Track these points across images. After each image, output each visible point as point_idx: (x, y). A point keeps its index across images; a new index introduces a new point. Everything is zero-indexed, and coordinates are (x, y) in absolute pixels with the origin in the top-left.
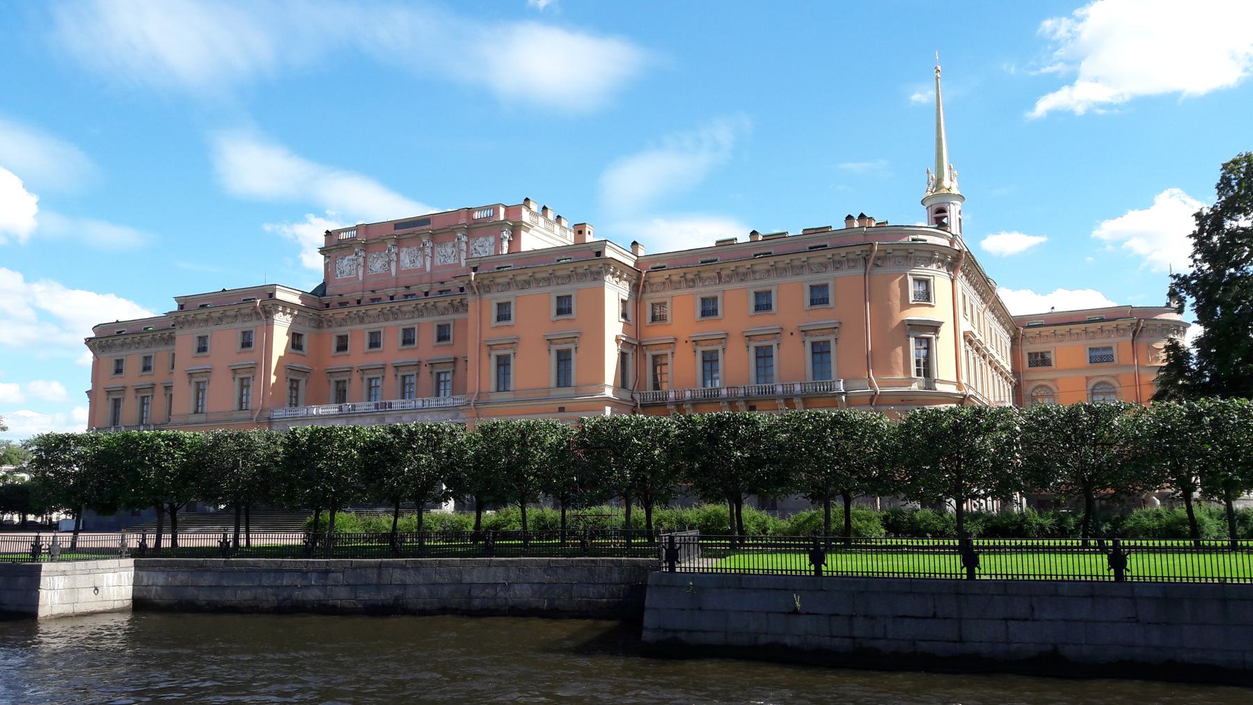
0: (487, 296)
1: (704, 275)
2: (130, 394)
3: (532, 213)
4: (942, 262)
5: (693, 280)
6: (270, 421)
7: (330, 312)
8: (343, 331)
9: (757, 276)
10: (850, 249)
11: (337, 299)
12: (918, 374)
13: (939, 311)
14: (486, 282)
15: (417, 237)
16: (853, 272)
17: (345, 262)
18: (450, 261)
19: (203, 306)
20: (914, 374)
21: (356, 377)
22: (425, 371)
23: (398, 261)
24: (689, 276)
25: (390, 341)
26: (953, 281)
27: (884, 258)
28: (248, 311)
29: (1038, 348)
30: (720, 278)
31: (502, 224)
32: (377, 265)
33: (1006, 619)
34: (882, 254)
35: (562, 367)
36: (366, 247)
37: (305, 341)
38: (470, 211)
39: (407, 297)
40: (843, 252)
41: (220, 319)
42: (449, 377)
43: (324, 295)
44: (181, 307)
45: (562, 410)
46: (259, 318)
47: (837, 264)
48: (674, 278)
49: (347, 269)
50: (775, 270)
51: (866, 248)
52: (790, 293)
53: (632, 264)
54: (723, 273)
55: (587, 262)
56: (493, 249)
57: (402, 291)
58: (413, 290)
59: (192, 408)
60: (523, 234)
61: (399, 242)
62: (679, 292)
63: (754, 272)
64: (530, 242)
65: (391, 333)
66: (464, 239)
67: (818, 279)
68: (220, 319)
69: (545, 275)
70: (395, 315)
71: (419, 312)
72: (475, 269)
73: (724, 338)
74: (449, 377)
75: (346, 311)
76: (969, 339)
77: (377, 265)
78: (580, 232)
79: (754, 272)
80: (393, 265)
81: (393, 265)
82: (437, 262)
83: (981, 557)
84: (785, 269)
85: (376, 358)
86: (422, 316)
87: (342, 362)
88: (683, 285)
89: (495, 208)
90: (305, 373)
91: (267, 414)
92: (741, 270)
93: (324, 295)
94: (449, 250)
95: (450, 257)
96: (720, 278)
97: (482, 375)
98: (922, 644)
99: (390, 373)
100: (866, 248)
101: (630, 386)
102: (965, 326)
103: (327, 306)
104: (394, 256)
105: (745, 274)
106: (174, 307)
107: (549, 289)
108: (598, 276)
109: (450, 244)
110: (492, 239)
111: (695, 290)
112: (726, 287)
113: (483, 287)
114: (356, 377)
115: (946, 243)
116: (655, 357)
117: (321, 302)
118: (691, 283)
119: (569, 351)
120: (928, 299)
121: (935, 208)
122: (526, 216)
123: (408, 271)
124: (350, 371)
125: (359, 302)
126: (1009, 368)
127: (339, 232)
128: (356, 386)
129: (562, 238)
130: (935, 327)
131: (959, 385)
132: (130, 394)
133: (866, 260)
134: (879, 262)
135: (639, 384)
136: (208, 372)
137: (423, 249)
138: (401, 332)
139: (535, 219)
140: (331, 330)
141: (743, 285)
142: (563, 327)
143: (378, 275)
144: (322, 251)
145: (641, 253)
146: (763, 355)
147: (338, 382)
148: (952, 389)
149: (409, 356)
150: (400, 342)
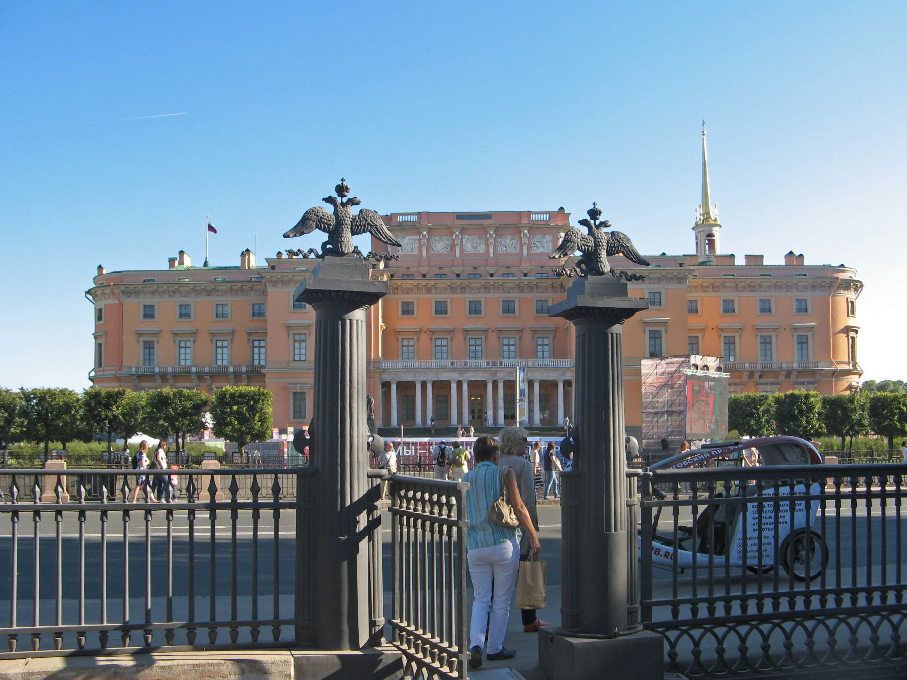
9: (763, 289)
11: (402, 271)
18: (511, 250)
24: (716, 284)
38: (529, 213)
44: (273, 268)
50: (777, 287)
57: (470, 270)
61: (463, 231)
62: (707, 294)
65: (458, 302)
70: (463, 289)
71: (487, 288)
77: (440, 246)
85: (441, 323)
86: (489, 292)
109: (509, 237)
111: (719, 294)
112: (741, 294)
118: (716, 288)
123: (470, 255)
140: (397, 296)
143: (441, 255)
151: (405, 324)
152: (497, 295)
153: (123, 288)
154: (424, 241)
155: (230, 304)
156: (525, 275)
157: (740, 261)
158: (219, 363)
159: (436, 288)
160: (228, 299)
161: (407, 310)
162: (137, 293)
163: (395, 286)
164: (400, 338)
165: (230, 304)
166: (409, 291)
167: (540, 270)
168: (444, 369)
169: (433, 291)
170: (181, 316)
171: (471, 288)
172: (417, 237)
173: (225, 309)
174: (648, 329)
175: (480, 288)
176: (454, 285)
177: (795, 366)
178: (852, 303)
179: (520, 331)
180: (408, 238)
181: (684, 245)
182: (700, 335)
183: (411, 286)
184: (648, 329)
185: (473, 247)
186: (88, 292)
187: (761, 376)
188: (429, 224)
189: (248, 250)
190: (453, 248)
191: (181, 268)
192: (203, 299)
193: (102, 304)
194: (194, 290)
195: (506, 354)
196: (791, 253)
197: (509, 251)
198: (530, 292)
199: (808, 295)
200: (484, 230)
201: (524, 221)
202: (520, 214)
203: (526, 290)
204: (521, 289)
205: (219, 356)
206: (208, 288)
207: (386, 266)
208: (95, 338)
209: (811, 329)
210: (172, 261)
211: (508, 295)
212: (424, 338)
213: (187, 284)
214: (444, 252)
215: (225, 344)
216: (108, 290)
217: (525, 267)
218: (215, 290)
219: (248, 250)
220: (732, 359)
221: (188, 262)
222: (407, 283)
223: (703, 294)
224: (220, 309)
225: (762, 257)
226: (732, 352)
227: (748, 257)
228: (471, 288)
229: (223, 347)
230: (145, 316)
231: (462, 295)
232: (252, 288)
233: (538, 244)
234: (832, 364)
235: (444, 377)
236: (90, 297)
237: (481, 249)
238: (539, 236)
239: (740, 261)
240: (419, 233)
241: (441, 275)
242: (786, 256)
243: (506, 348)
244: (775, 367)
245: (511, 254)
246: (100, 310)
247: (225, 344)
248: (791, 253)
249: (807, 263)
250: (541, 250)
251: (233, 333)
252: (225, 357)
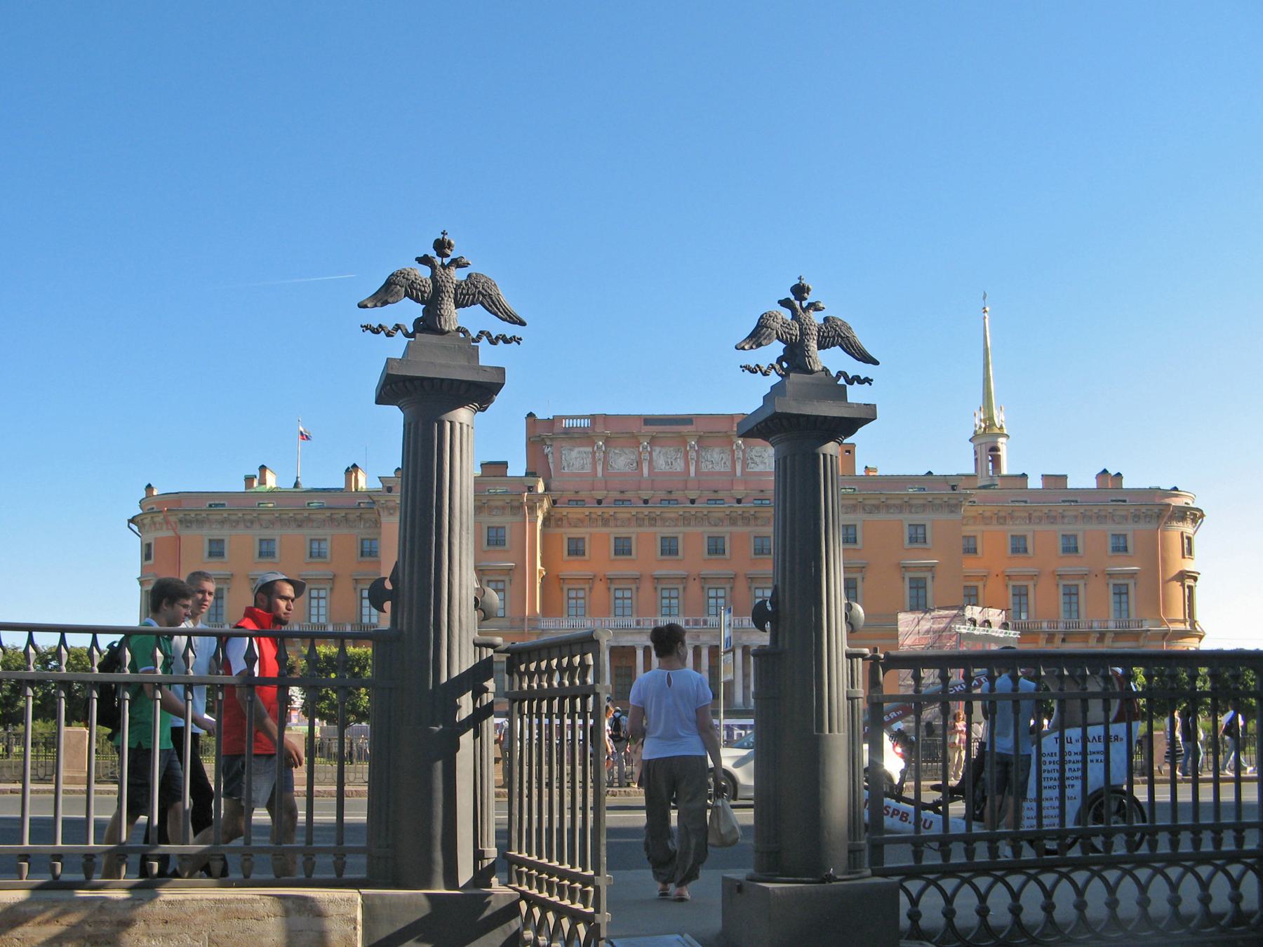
9: (1066, 520)
17: (574, 454)
18: (720, 468)
24: (1002, 514)
50: (1086, 518)
57: (662, 494)
61: (653, 441)
62: (988, 528)
65: (646, 539)
70: (653, 520)
71: (686, 520)
77: (621, 461)
85: (623, 568)
86: (689, 525)
107: (900, 516)
109: (717, 450)
111: (1006, 527)
112: (1037, 528)
118: (1002, 520)
123: (664, 474)
143: (624, 474)
151: (573, 568)
152: (700, 529)
153: (181, 515)
154: (600, 455)
155: (329, 538)
156: (739, 501)
157: (1035, 483)
158: (314, 619)
159: (616, 519)
160: (325, 532)
161: (576, 549)
162: (200, 522)
163: (558, 516)
164: (565, 588)
165: (329, 538)
166: (579, 523)
167: (760, 495)
168: (626, 629)
169: (612, 523)
170: (261, 554)
171: (664, 520)
172: (590, 449)
173: (323, 545)
174: (908, 575)
175: (677, 519)
176: (641, 516)
177: (1112, 625)
178: (1189, 539)
179: (733, 579)
180: (577, 450)
181: (959, 461)
182: (980, 585)
183: (581, 516)
184: (908, 575)
185: (667, 463)
186: (132, 521)
187: (1063, 640)
188: (607, 431)
189: (355, 466)
190: (639, 463)
191: (262, 488)
192: (292, 532)
193: (150, 537)
194: (280, 520)
195: (713, 610)
196: (1105, 471)
197: (717, 469)
198: (748, 525)
199: (1128, 528)
200: (682, 440)
203: (740, 522)
204: (733, 521)
205: (314, 611)
206: (299, 517)
207: (547, 488)
208: (142, 583)
209: (1132, 575)
210: (249, 480)
211: (715, 529)
212: (600, 587)
213: (271, 511)
214: (627, 469)
215: (323, 593)
216: (159, 518)
217: (739, 491)
218: (309, 520)
219: (355, 466)
220: (1024, 616)
221: (271, 481)
222: (575, 513)
224: (315, 545)
225: (1065, 477)
226: (1024, 608)
227: (1045, 477)
228: (664, 520)
229: (319, 598)
230: (211, 554)
231: (652, 529)
232: (360, 517)
234: (1162, 622)
235: (626, 641)
236: (135, 528)
237: (679, 466)
238: (757, 448)
239: (1035, 483)
240: (593, 443)
241: (623, 501)
242: (1098, 476)
243: (712, 601)
244: (1084, 628)
245: (720, 473)
246: (149, 546)
247: (323, 593)
248: (1105, 471)
249: (1126, 484)
250: (760, 468)
251: (333, 579)
252: (322, 611)
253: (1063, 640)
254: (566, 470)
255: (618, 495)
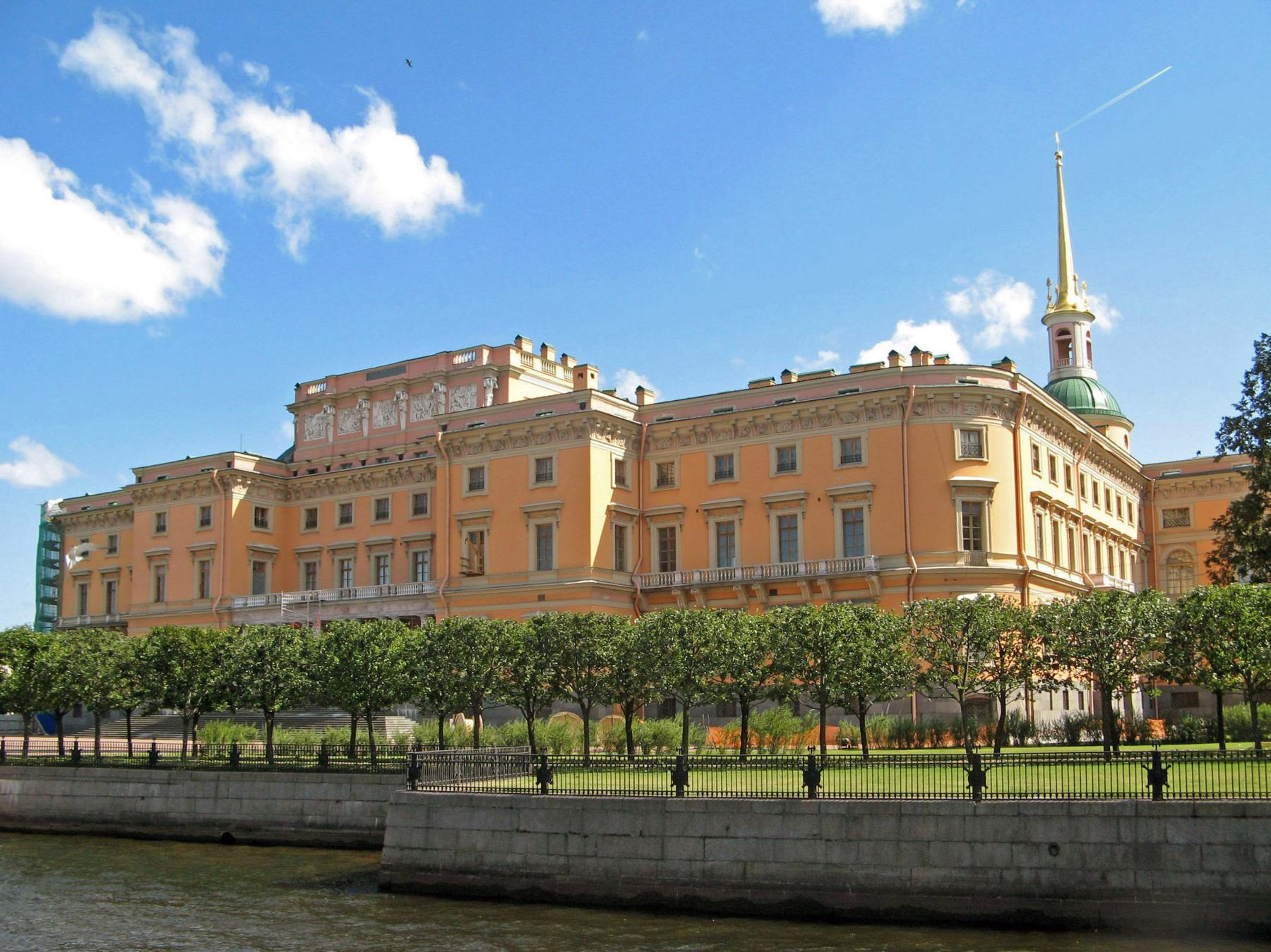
0: (457, 460)
1: (718, 427)
2: (96, 578)
3: (525, 355)
4: (1000, 407)
5: (705, 435)
6: (231, 612)
7: (298, 482)
8: (311, 503)
9: (779, 428)
10: (885, 395)
12: (967, 545)
13: (997, 468)
14: (456, 443)
15: (390, 389)
16: (889, 422)
17: (314, 421)
19: (161, 479)
20: (960, 548)
21: (325, 558)
22: (400, 550)
23: (370, 419)
24: (700, 429)
25: (364, 514)
26: (1015, 432)
27: (925, 404)
28: (206, 483)
29: (1176, 503)
30: (736, 431)
31: (485, 369)
32: (348, 425)
33: (704, 838)
34: (922, 400)
35: (543, 542)
36: (336, 401)
37: (270, 518)
38: (450, 355)
39: (382, 461)
40: (876, 398)
41: (178, 493)
42: (427, 557)
43: (292, 461)
44: (139, 480)
45: (542, 598)
46: (217, 492)
47: (871, 413)
48: (683, 432)
49: (316, 429)
51: (904, 392)
52: (817, 446)
53: (630, 416)
54: (740, 424)
55: (572, 417)
56: (475, 400)
57: (375, 454)
58: (386, 453)
59: (152, 596)
60: (511, 380)
63: (775, 423)
64: (518, 391)
66: (442, 389)
67: (848, 431)
68: (178, 493)
69: (522, 433)
70: (367, 482)
71: (392, 478)
72: (444, 428)
73: (739, 507)
74: (427, 557)
75: (314, 479)
76: (1039, 499)
78: (581, 375)
79: (775, 423)
80: (365, 422)
81: (365, 422)
82: (413, 419)
83: (690, 774)
84: (811, 419)
85: (346, 538)
86: (396, 484)
87: (309, 542)
88: (694, 440)
89: (478, 350)
90: (270, 554)
91: (227, 604)
92: (759, 421)
93: (292, 461)
94: (427, 403)
95: (423, 411)
96: (736, 431)
97: (452, 552)
98: (629, 862)
99: (362, 553)
100: (904, 392)
101: (630, 565)
102: (1031, 483)
103: (295, 474)
104: (366, 414)
105: (765, 426)
106: (132, 480)
108: (582, 434)
109: (428, 396)
110: (474, 389)
112: (744, 442)
113: (451, 449)
114: (325, 558)
115: (1005, 385)
116: (662, 531)
117: (288, 469)
118: (703, 437)
119: (550, 526)
120: (980, 455)
121: (1057, 328)
122: (515, 359)
124: (320, 551)
125: (328, 468)
126: (1132, 532)
127: (308, 385)
128: (327, 568)
129: (560, 383)
130: (988, 489)
131: (1020, 558)
132: (96, 578)
133: (903, 408)
134: (920, 410)
135: (643, 564)
136: (165, 555)
137: (397, 403)
138: (373, 504)
139: (527, 361)
140: (300, 502)
141: (763, 439)
142: (543, 498)
144: (291, 408)
145: (648, 400)
146: (787, 527)
147: (308, 565)
148: (1012, 565)
149: (382, 534)
150: (373, 516)
201: (442, 367)
202: (436, 356)
223: (681, 450)
233: (460, 401)
237: (393, 422)
253: (773, 592)
254: (308, 439)
255: (343, 461)
